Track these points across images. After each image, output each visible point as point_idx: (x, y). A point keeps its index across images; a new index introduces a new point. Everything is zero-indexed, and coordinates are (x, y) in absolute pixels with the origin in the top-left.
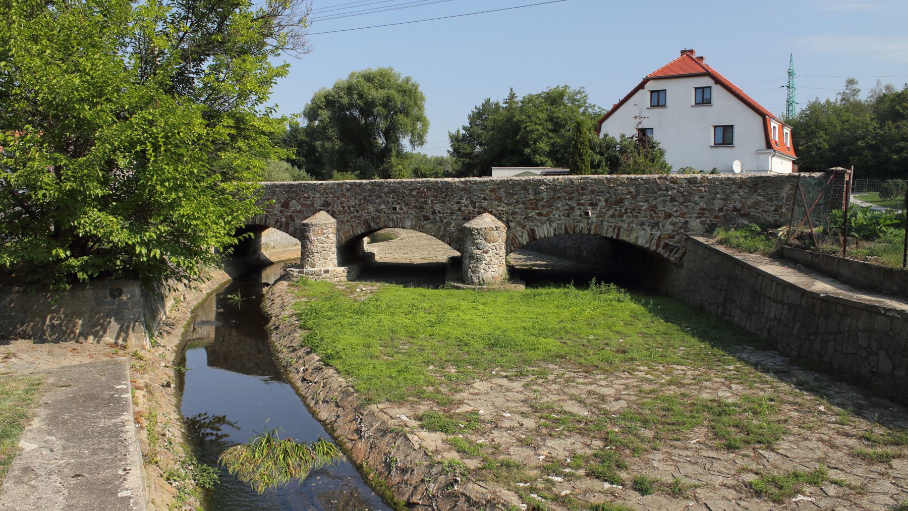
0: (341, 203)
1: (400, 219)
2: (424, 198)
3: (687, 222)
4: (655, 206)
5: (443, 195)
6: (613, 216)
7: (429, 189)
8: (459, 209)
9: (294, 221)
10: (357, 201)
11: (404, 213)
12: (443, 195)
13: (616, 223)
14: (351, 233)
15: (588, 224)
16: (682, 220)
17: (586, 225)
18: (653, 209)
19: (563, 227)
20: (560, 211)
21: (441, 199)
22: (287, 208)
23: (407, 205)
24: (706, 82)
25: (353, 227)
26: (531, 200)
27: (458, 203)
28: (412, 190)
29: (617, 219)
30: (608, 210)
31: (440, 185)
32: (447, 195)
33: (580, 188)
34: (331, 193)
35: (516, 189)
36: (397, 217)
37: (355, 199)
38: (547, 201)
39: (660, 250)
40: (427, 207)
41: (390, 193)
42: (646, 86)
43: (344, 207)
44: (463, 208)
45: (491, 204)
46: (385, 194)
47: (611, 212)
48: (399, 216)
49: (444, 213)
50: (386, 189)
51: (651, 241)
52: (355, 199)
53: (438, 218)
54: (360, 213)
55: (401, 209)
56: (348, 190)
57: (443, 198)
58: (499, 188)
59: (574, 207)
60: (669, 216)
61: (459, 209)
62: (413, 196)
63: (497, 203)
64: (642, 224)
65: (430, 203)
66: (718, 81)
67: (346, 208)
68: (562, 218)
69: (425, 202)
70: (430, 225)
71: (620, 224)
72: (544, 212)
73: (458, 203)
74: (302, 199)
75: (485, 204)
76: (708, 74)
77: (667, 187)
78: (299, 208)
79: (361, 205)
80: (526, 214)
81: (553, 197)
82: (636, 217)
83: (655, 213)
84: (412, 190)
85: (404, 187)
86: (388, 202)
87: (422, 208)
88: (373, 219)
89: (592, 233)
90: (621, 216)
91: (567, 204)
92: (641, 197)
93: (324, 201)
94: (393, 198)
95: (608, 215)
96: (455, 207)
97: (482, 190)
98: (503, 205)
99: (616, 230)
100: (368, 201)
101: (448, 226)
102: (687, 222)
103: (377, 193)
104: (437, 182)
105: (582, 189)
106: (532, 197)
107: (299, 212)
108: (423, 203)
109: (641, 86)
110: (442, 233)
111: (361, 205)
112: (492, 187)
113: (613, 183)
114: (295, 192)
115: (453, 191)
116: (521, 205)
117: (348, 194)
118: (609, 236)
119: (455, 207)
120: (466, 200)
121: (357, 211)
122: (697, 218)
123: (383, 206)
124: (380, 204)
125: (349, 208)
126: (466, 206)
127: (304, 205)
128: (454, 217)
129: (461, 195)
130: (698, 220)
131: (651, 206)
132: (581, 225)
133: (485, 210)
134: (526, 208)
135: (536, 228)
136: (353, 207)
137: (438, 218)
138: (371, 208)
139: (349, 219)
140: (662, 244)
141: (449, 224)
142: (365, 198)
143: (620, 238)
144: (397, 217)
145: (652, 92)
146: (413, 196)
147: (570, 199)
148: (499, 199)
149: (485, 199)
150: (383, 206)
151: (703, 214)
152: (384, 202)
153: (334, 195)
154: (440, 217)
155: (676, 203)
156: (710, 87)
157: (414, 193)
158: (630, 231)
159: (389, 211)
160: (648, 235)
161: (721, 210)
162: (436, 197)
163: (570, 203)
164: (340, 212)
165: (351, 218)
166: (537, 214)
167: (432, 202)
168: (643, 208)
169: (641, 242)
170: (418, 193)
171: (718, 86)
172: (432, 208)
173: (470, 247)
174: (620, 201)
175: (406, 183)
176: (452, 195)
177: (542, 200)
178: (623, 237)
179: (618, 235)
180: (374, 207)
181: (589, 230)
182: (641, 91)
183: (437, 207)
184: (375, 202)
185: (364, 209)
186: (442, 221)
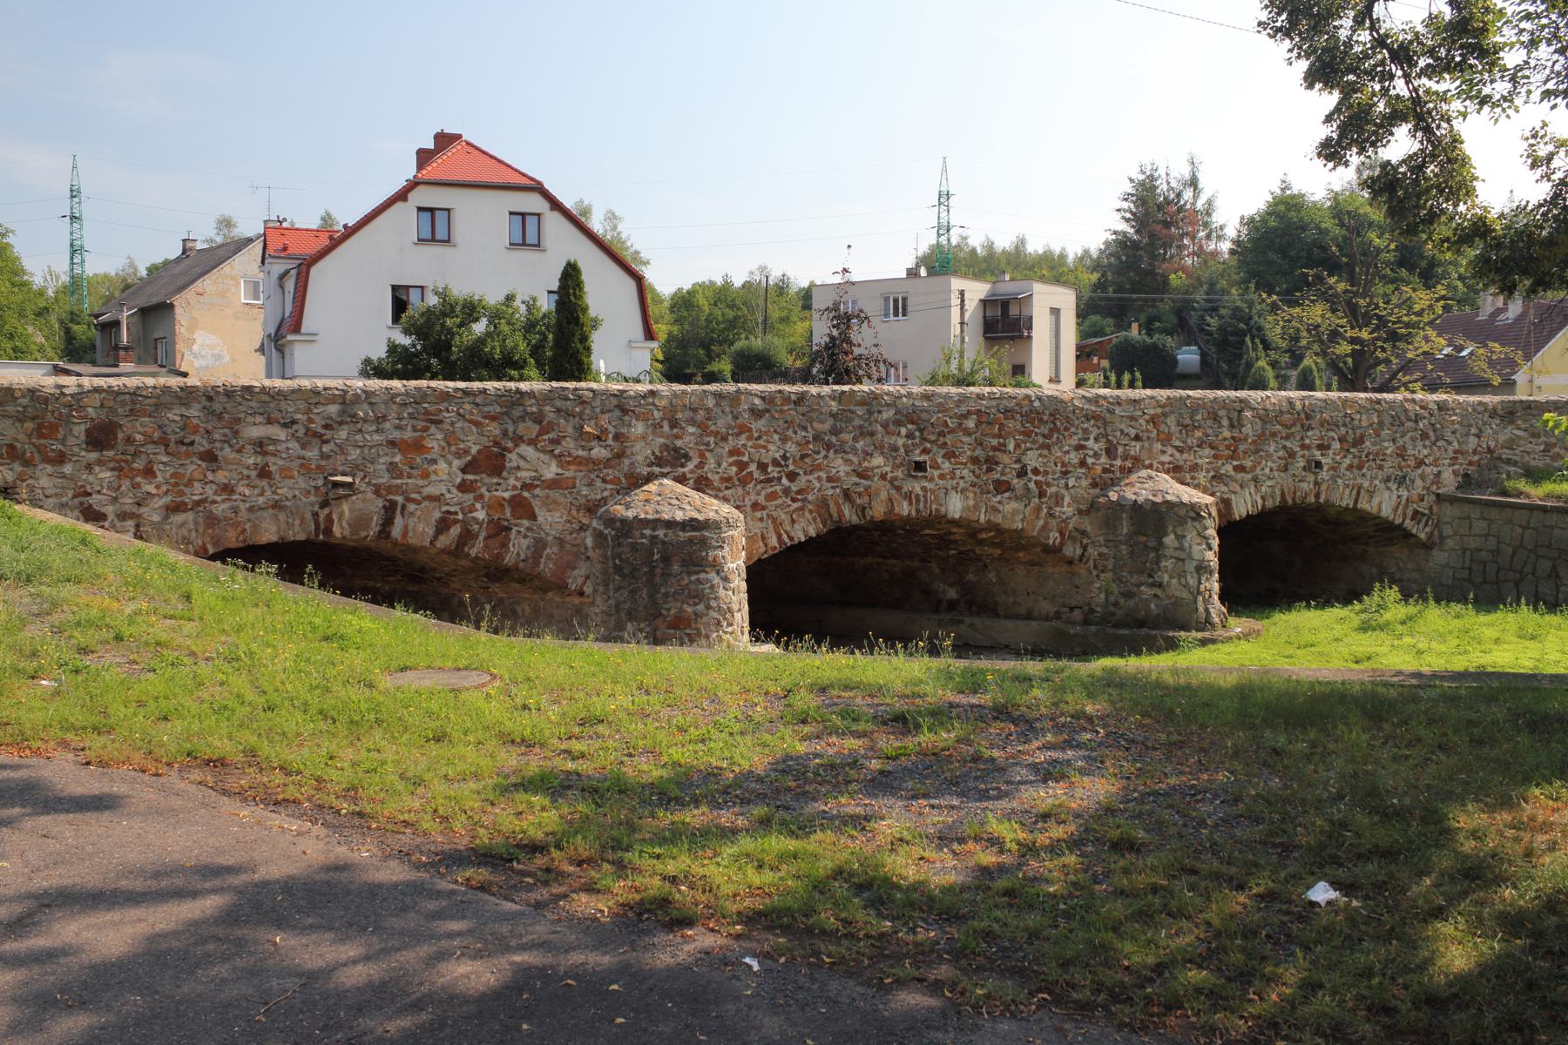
0: (732, 453)
1: (933, 492)
2: (999, 436)
3: (1439, 472)
4: (1404, 448)
5: (1045, 429)
6: (1350, 467)
7: (1008, 412)
8: (1083, 463)
9: (533, 517)
10: (791, 448)
11: (942, 477)
12: (1045, 429)
13: (1355, 479)
14: (773, 541)
15: (1316, 483)
16: (1435, 470)
17: (1312, 486)
18: (1401, 453)
19: (1278, 492)
20: (1273, 462)
21: (1041, 440)
22: (499, 475)
23: (949, 455)
24: (534, 203)
25: (777, 524)
26: (1225, 439)
27: (1079, 447)
28: (966, 416)
29: (1356, 471)
30: (1345, 457)
31: (1037, 404)
32: (1055, 429)
33: (1303, 416)
34: (692, 422)
35: (1199, 417)
36: (924, 489)
37: (784, 440)
38: (1254, 442)
39: (1408, 524)
40: (1005, 459)
41: (898, 423)
42: (410, 196)
43: (742, 466)
44: (1090, 461)
45: (1150, 450)
46: (885, 426)
47: (1347, 461)
48: (929, 485)
49: (1046, 473)
50: (888, 414)
51: (1397, 507)
52: (784, 440)
53: (1032, 485)
54: (802, 480)
55: (936, 466)
56: (756, 413)
57: (1044, 436)
58: (1165, 415)
59: (1295, 453)
60: (1420, 463)
61: (1083, 463)
62: (967, 432)
63: (1160, 447)
64: (1388, 480)
65: (1011, 447)
66: (556, 205)
67: (753, 467)
68: (1276, 474)
69: (1001, 448)
70: (1014, 505)
71: (1359, 481)
72: (1248, 463)
73: (1079, 447)
74: (569, 444)
75: (1135, 448)
76: (538, 189)
77: (1416, 415)
78: (551, 471)
79: (803, 457)
80: (1216, 470)
81: (1263, 434)
82: (1380, 468)
83: (1404, 460)
84: (966, 416)
85: (942, 409)
86: (895, 449)
87: (991, 463)
88: (847, 495)
89: (1322, 501)
90: (1360, 467)
91: (1284, 447)
92: (1386, 433)
93: (665, 447)
94: (910, 436)
95: (1344, 465)
96: (1074, 457)
97: (1132, 418)
98: (1170, 450)
99: (1355, 492)
100: (829, 446)
101: (1057, 504)
102: (1439, 472)
103: (857, 422)
104: (1028, 397)
105: (1308, 417)
106: (1227, 434)
107: (554, 484)
108: (995, 449)
109: (402, 196)
110: (1041, 522)
111: (803, 457)
112: (1152, 412)
113: (1351, 407)
114: (538, 419)
115: (1068, 420)
116: (1207, 451)
117: (759, 425)
118: (1344, 504)
119: (1074, 457)
120: (1096, 439)
121: (792, 476)
122: (1450, 465)
123: (878, 460)
124: (868, 455)
125: (762, 467)
126: (1096, 455)
127: (578, 461)
128: (1071, 482)
129: (1085, 431)
130: (1450, 469)
131: (1398, 448)
132: (1304, 485)
133: (1138, 463)
134: (1215, 457)
135: (1233, 497)
136: (776, 463)
137: (1032, 485)
138: (840, 466)
139: (761, 499)
140: (1410, 512)
141: (1058, 499)
142: (817, 438)
143: (1359, 506)
144: (924, 489)
145: (420, 209)
146: (967, 432)
147: (1287, 438)
148: (1166, 439)
149: (1137, 438)
150: (878, 460)
151: (1457, 458)
152: (879, 448)
153: (703, 427)
154: (1036, 482)
155: (1427, 443)
156: (538, 215)
157: (971, 424)
158: (1371, 493)
159: (899, 474)
160: (1395, 497)
161: (1475, 452)
162: (1027, 434)
163: (1288, 444)
164: (729, 479)
165: (772, 496)
166: (1236, 468)
167: (1017, 446)
168: (1388, 452)
169: (1386, 512)
170: (979, 423)
171: (556, 215)
172: (1018, 461)
173: (1196, 549)
174: (1359, 441)
175: (947, 397)
176: (1066, 429)
177: (1246, 439)
178: (1363, 505)
179: (1356, 501)
180: (847, 461)
181: (1317, 496)
182: (399, 205)
183: (1032, 459)
184: (854, 450)
185: (819, 468)
186: (1042, 494)
